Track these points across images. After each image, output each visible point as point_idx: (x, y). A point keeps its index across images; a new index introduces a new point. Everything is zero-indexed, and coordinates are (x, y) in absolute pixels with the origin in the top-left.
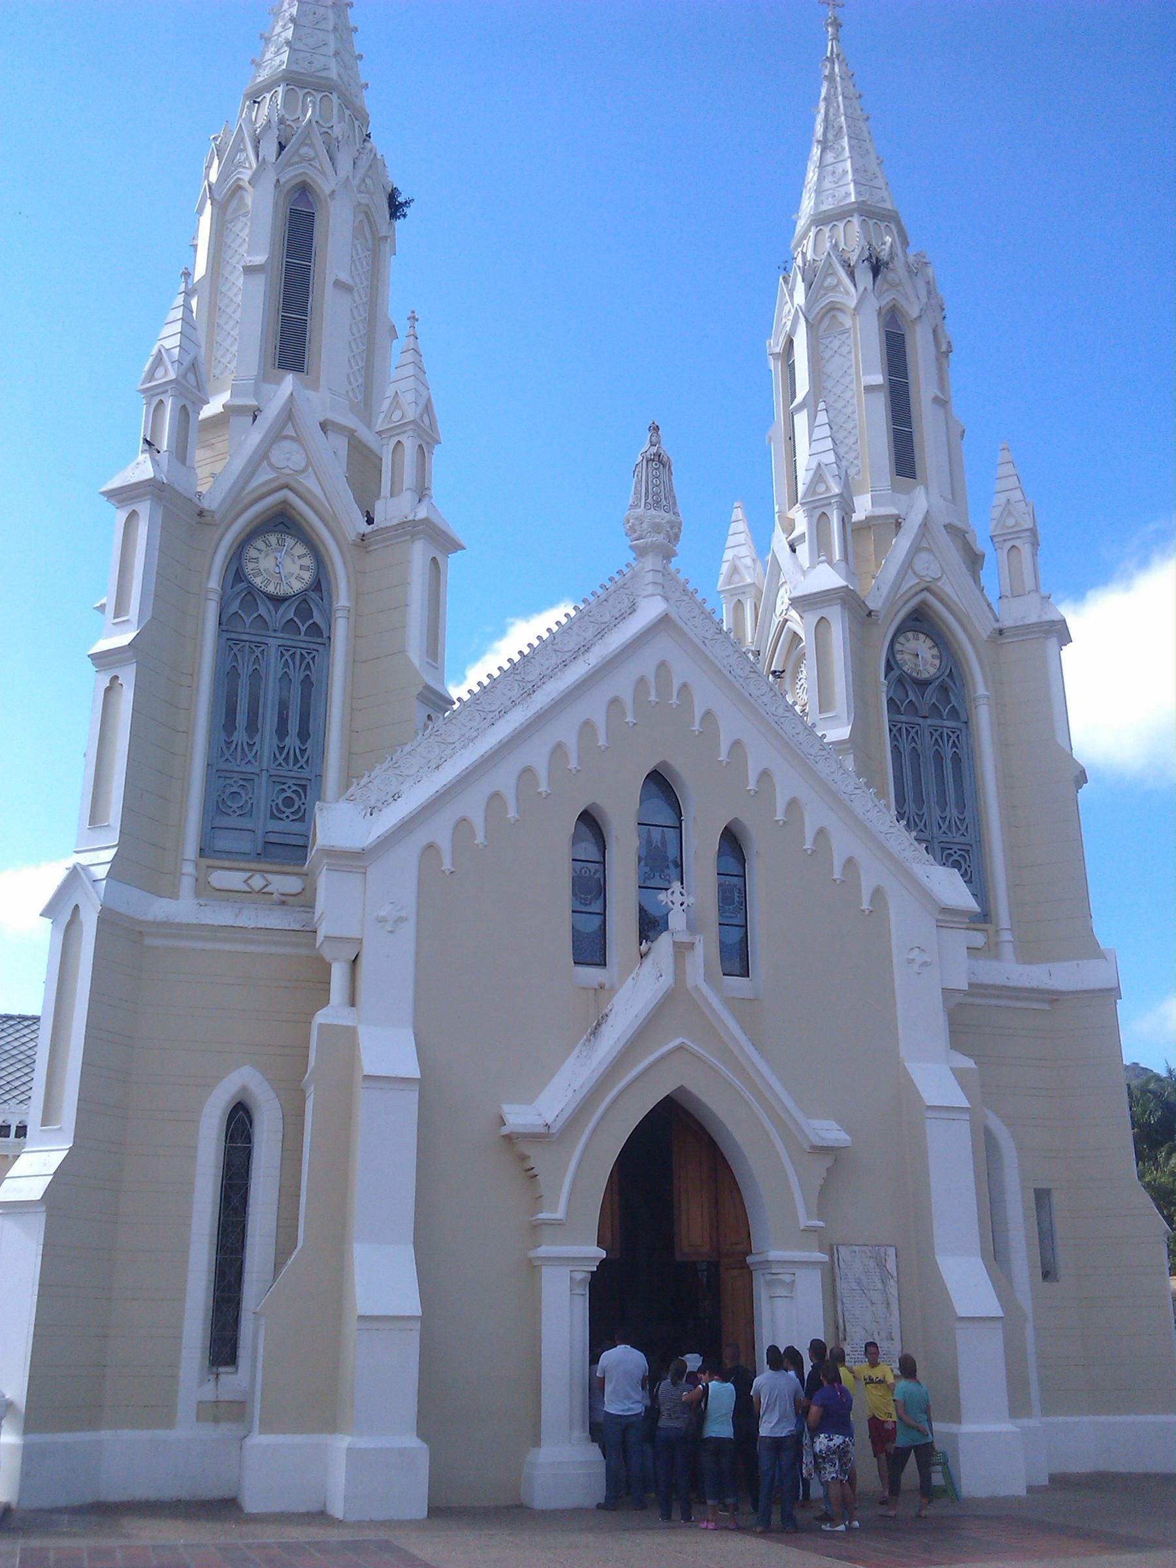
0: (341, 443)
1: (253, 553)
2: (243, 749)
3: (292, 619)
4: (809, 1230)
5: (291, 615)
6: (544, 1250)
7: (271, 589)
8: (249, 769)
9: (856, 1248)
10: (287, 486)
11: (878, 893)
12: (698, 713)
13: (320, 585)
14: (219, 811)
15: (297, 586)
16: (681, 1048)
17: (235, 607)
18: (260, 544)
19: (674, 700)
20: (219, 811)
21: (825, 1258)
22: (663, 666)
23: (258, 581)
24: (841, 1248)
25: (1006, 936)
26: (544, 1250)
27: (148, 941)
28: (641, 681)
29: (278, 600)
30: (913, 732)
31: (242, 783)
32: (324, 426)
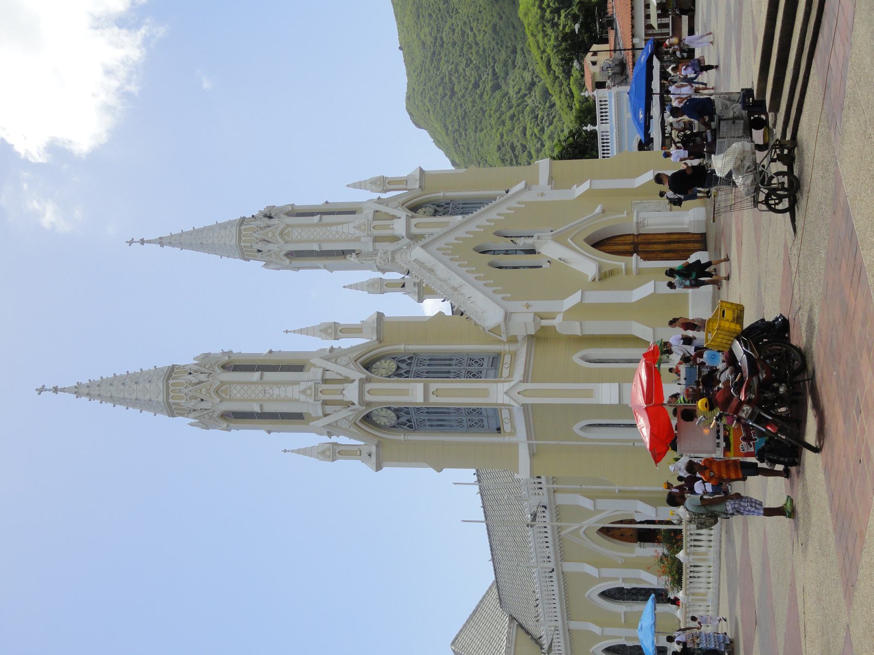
0: (329, 409)
1: (382, 423)
2: (459, 422)
3: (404, 413)
5: (402, 413)
7: (395, 418)
8: (465, 421)
10: (355, 423)
13: (389, 408)
14: (483, 427)
15: (389, 412)
17: (405, 427)
18: (378, 422)
20: (483, 427)
23: (393, 422)
27: (535, 451)
29: (398, 418)
31: (471, 422)
32: (325, 415)
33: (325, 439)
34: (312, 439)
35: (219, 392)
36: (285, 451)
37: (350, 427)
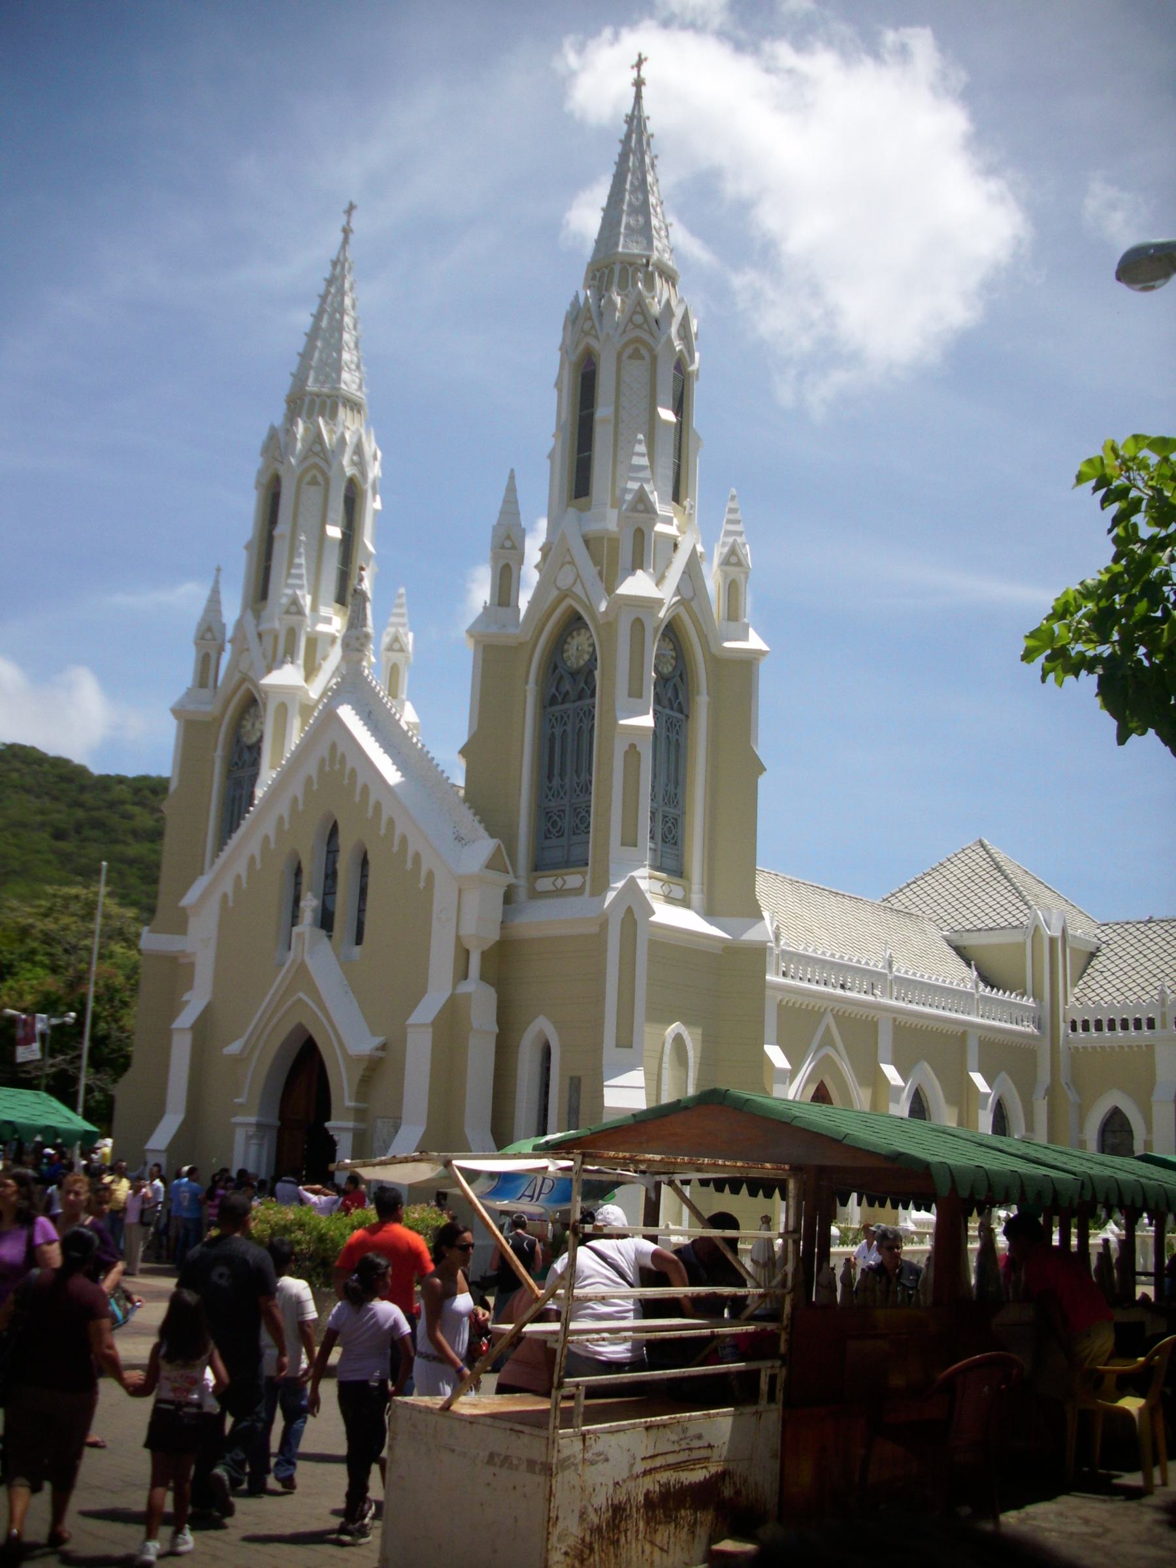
1: (245, 723)
4: (348, 1109)
6: (234, 1120)
9: (385, 1120)
11: (430, 875)
12: (347, 771)
16: (300, 1000)
19: (337, 766)
21: (351, 1124)
22: (334, 747)
24: (379, 1122)
25: (588, 877)
26: (234, 1120)
28: (323, 761)
30: (565, 718)
32: (260, 636)
33: (229, 633)
34: (231, 611)
35: (314, 472)
36: (218, 570)
37: (240, 672)
